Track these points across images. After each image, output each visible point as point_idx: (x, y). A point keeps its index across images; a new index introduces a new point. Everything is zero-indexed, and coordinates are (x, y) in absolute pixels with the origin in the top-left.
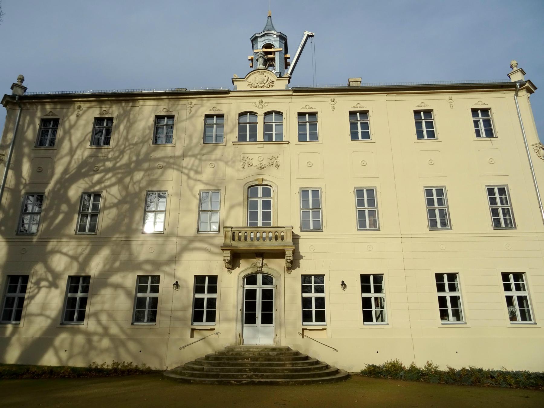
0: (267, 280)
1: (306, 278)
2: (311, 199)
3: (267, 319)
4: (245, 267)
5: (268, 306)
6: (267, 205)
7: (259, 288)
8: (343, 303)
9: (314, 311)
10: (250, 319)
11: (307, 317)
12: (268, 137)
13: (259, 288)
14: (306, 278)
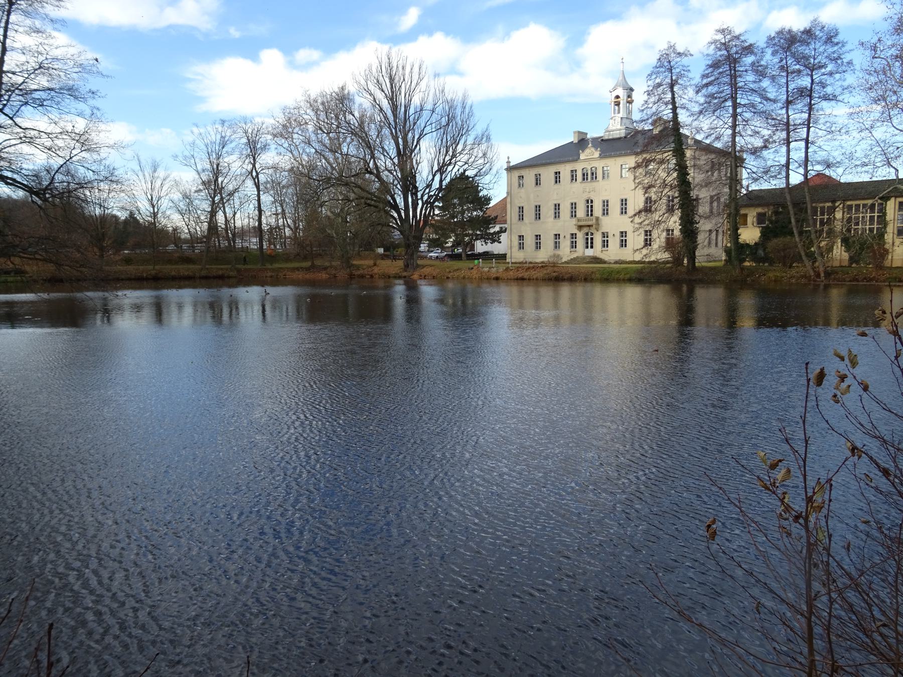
0: (592, 234)
1: (603, 233)
2: (606, 203)
3: (592, 247)
4: (585, 230)
5: (592, 243)
6: (592, 206)
7: (589, 237)
8: (614, 242)
9: (605, 244)
10: (587, 247)
11: (604, 246)
12: (592, 179)
13: (589, 237)
14: (603, 233)
